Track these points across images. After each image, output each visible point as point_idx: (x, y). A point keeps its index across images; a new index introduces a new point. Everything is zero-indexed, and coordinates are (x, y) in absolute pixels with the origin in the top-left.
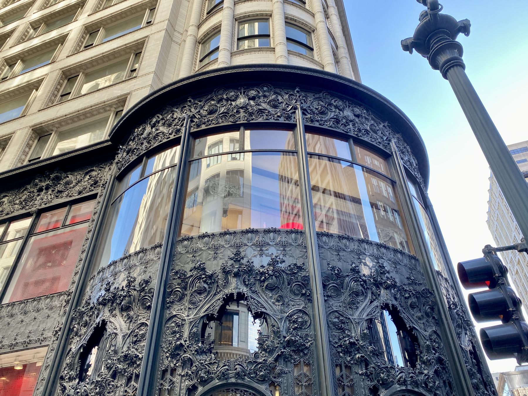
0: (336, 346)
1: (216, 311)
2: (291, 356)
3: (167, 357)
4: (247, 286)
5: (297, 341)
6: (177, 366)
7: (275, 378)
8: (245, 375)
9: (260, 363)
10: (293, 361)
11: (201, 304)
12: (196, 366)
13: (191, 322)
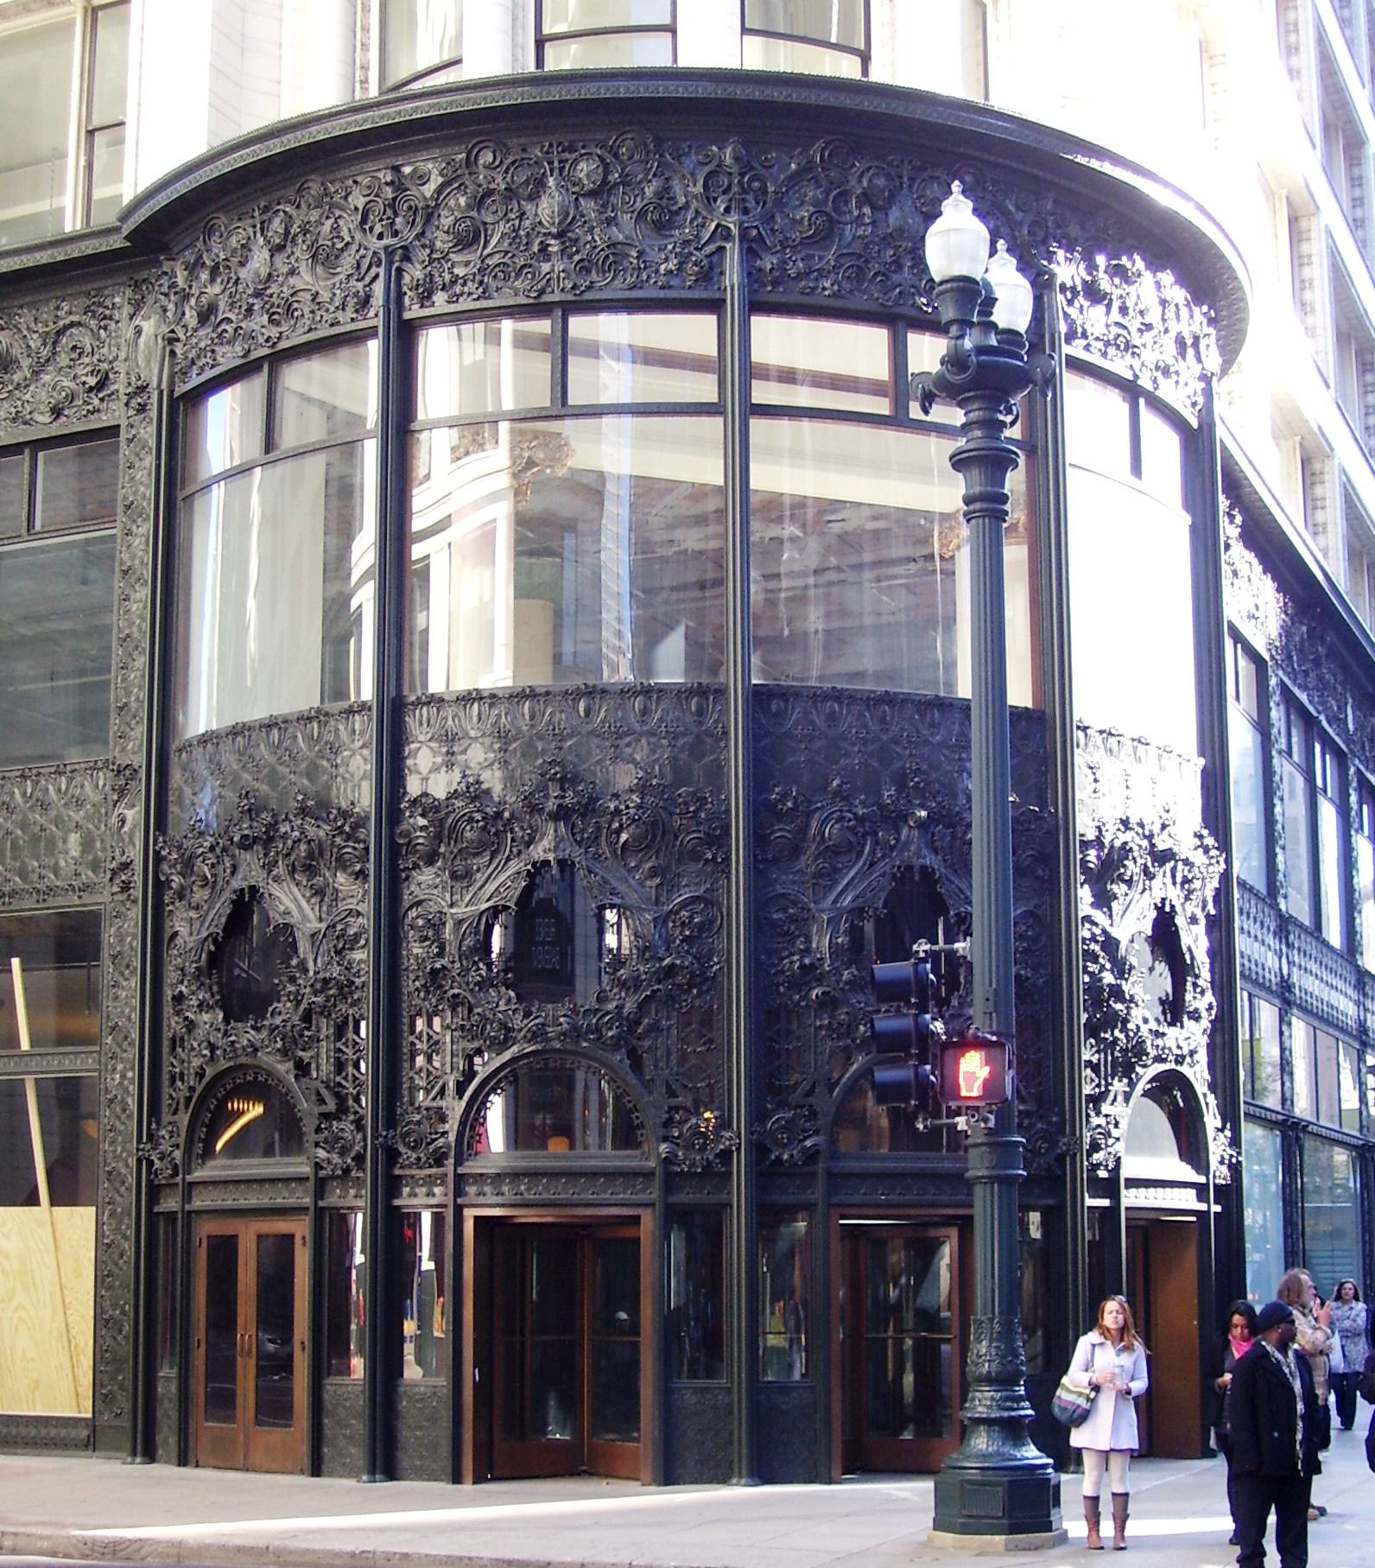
1: (515, 899)
4: (579, 843)
9: (608, 1013)
11: (480, 877)
13: (461, 922)
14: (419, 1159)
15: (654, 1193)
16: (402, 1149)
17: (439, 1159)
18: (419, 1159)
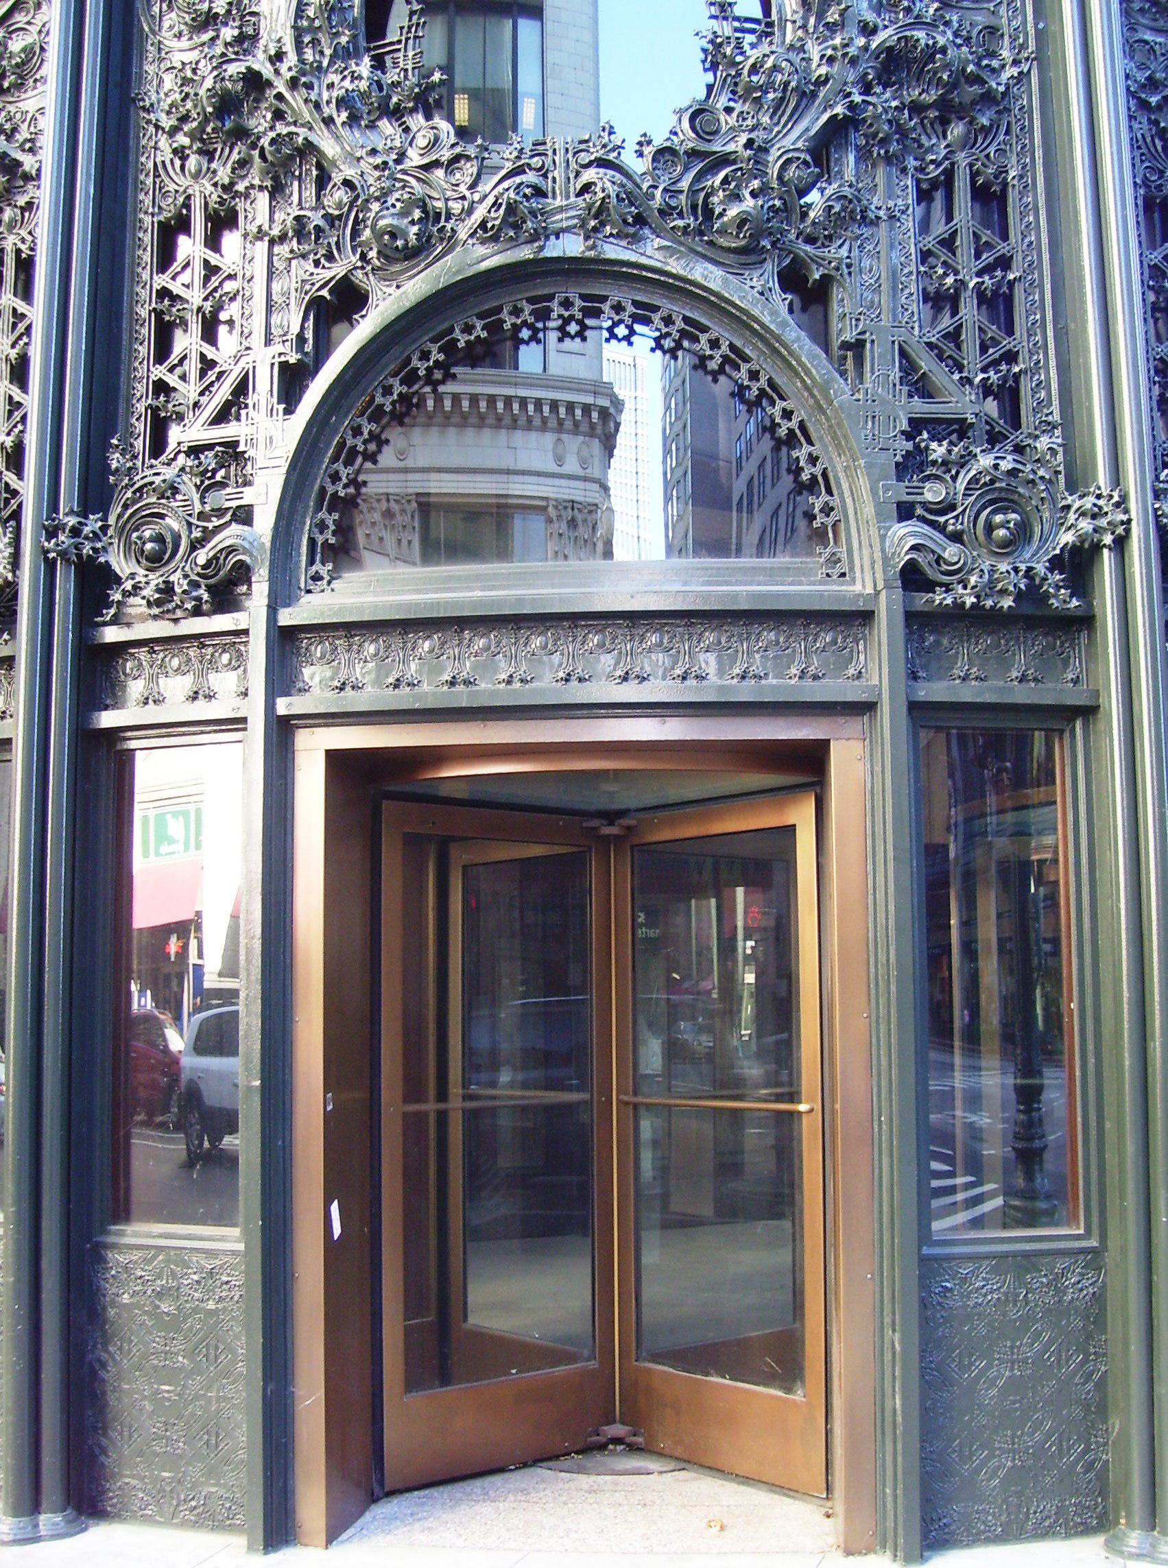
0: (1154, 100)
2: (903, 133)
3: (180, 153)
5: (943, 50)
6: (237, 194)
7: (811, 240)
8: (640, 220)
10: (911, 163)
12: (347, 183)
14: (167, 590)
15: (876, 666)
16: (121, 564)
17: (225, 590)
18: (167, 590)
